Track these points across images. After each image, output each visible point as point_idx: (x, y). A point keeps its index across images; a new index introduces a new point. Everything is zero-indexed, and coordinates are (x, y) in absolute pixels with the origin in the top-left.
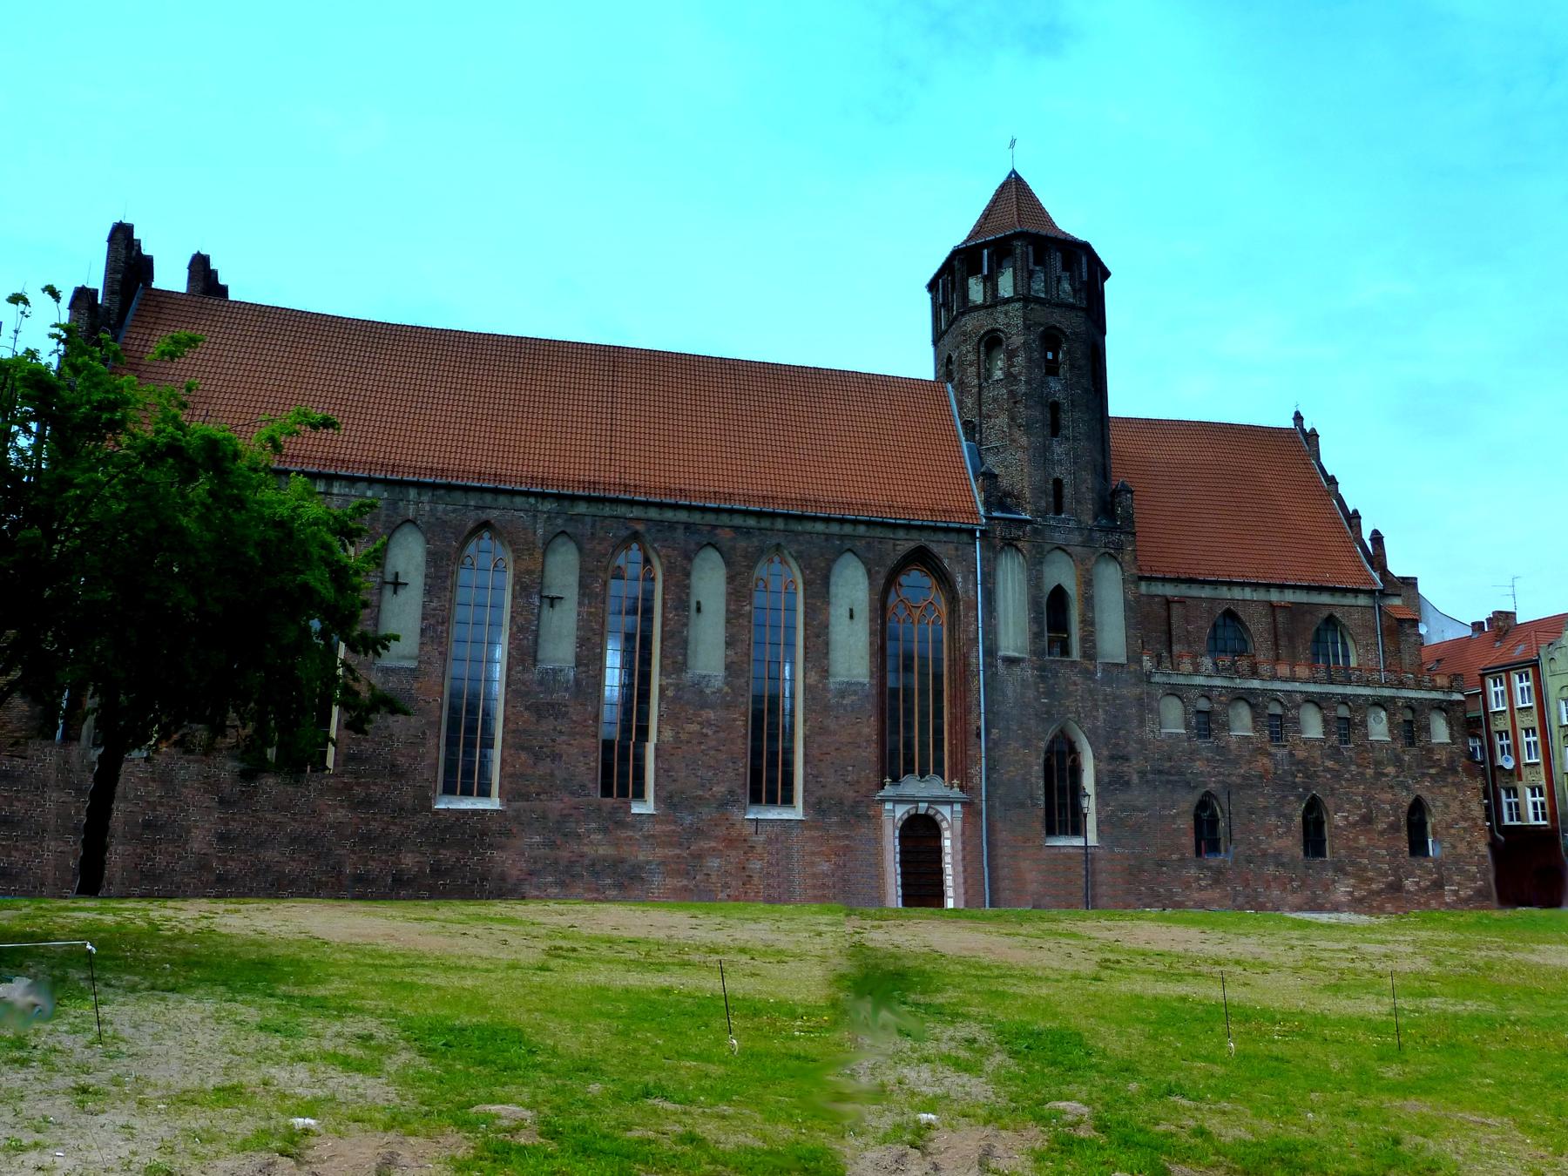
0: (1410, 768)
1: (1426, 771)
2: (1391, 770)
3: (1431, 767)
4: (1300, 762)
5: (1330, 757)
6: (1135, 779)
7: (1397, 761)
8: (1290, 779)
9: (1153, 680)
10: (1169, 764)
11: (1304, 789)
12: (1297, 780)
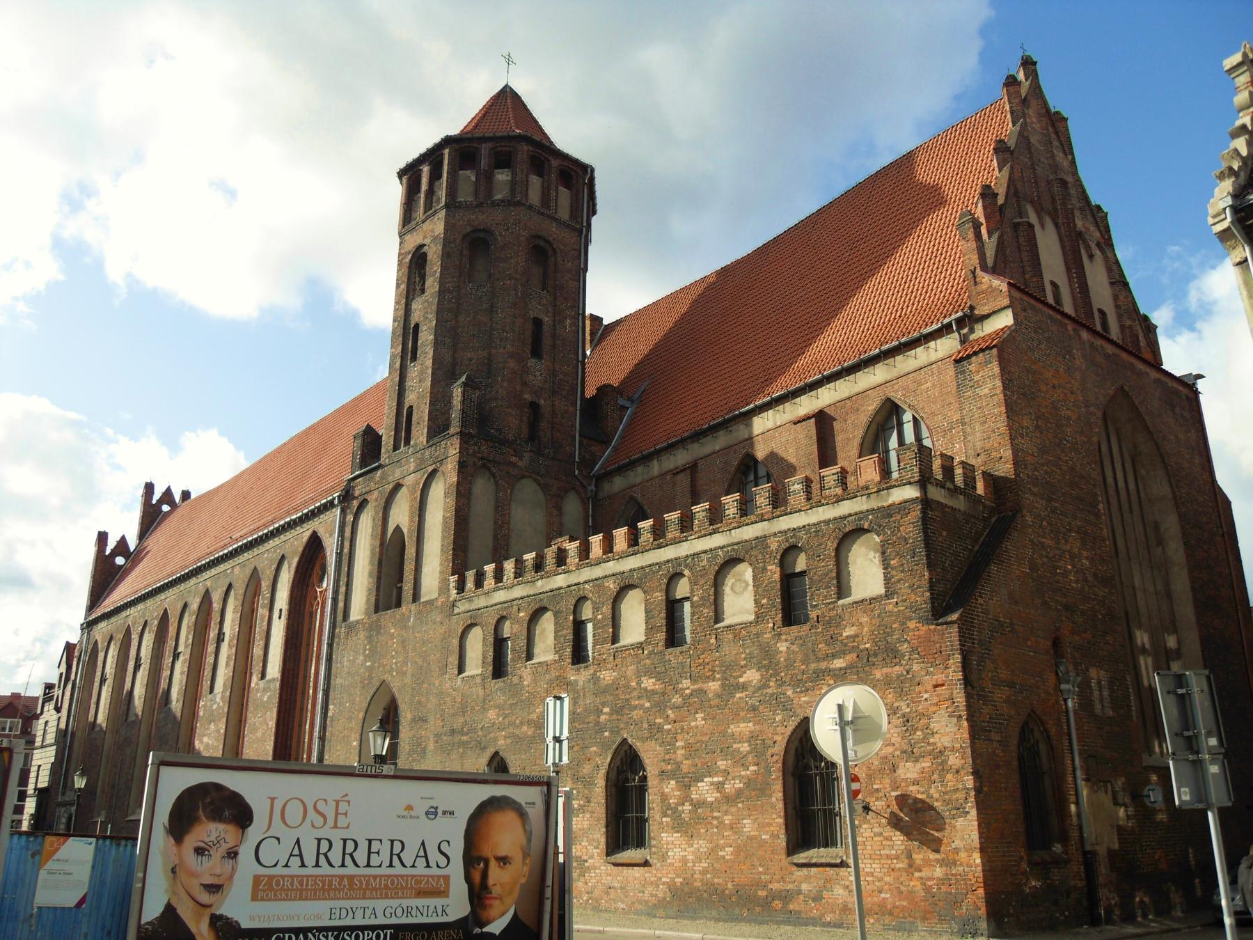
0: (790, 664)
1: (823, 665)
2: (752, 676)
3: (834, 656)
4: (606, 690)
5: (649, 672)
6: (431, 746)
7: (767, 660)
8: (592, 718)
9: (456, 610)
10: (461, 720)
11: (612, 732)
12: (603, 718)
